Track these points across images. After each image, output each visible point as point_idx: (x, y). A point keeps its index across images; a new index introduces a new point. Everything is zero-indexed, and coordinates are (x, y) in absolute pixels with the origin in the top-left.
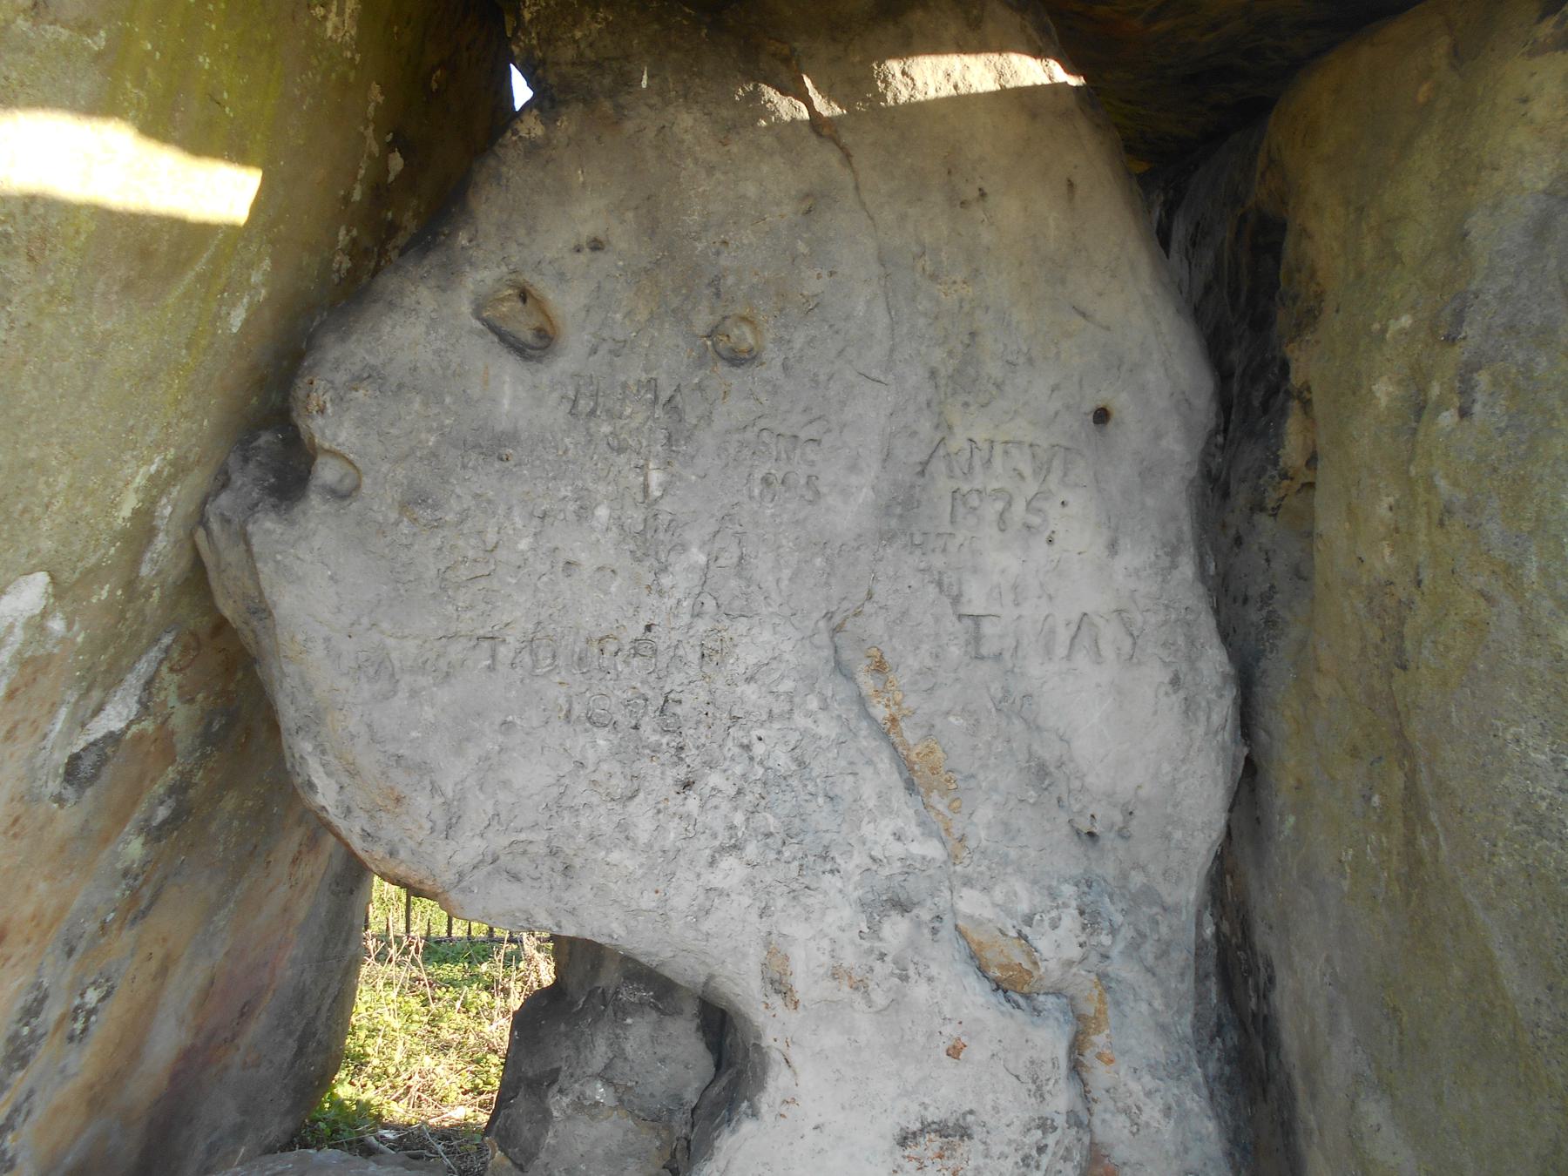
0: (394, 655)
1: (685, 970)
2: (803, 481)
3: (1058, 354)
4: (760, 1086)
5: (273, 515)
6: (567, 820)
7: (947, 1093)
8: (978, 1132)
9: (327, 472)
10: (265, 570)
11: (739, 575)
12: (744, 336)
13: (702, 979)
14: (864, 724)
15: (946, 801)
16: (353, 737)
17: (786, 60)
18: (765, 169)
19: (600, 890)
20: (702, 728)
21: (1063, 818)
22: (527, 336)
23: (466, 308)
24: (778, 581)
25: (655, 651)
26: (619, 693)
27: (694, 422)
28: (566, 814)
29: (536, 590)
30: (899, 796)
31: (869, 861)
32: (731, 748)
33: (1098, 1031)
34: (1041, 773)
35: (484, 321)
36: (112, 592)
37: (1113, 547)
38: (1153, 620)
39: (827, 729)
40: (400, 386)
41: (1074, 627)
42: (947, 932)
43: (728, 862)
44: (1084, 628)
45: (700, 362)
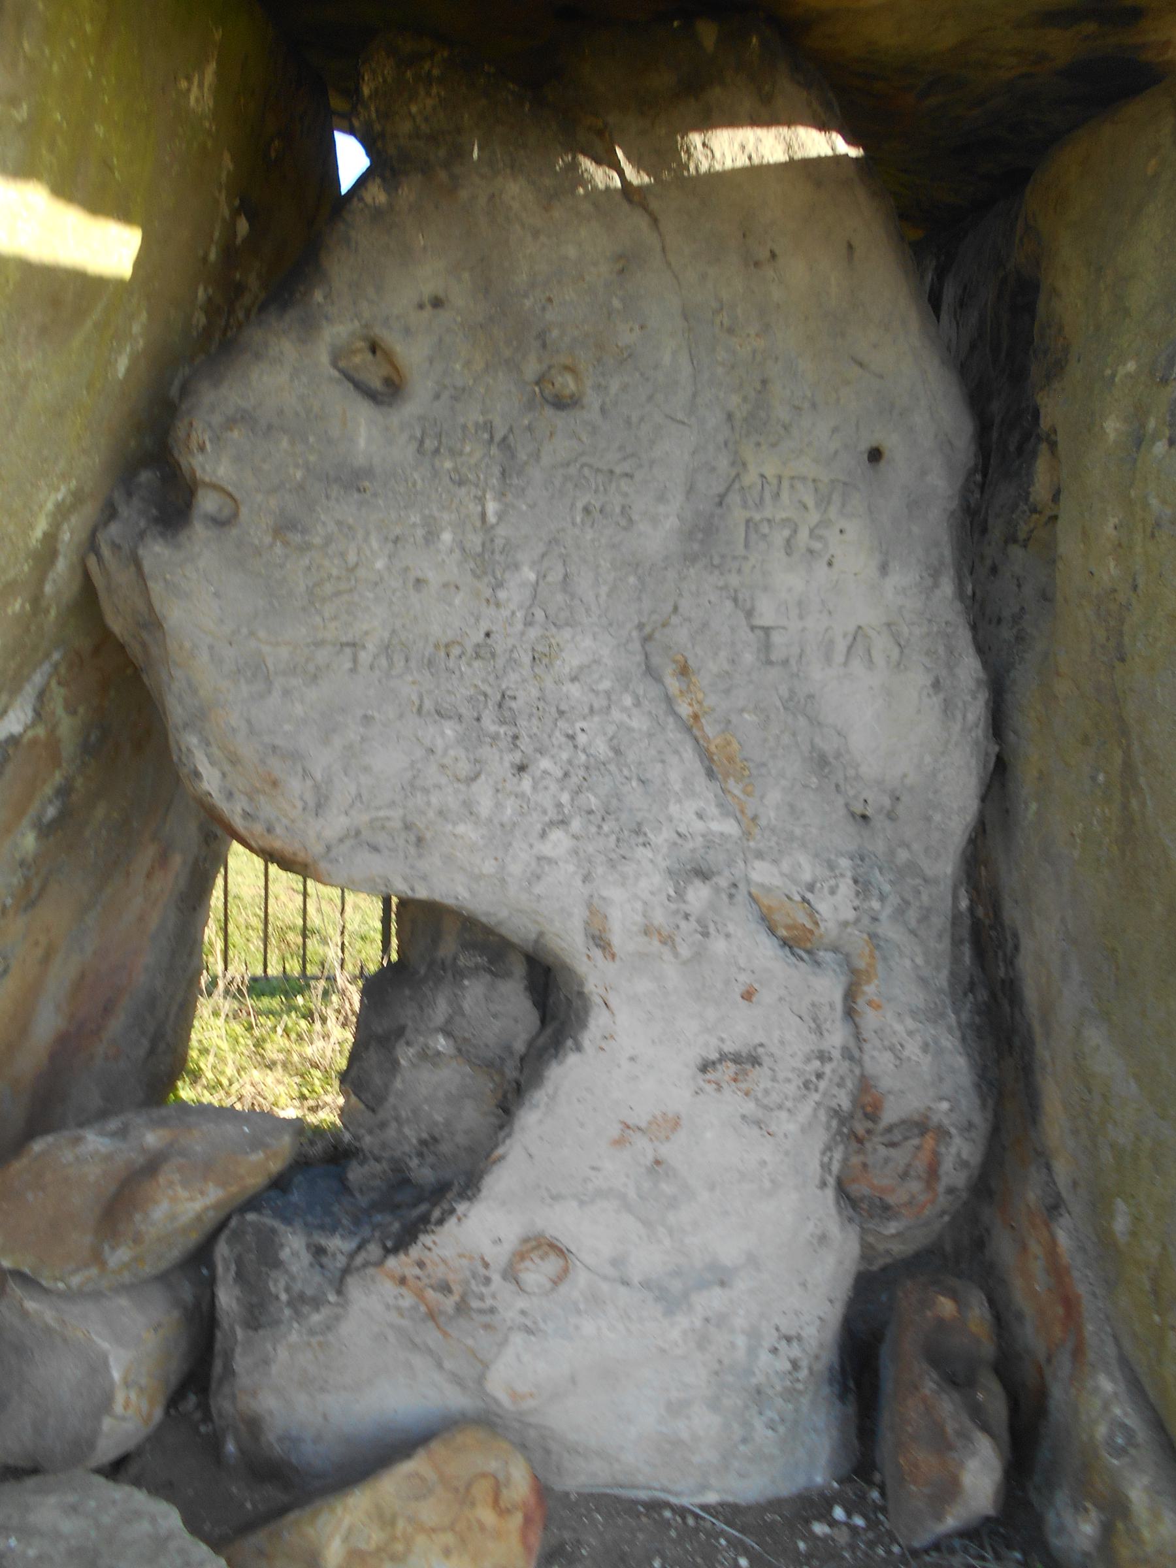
0: (270, 662)
1: (520, 929)
2: (618, 510)
3: (838, 399)
4: (583, 1024)
5: (160, 540)
6: (420, 799)
7: (741, 1030)
8: (766, 1061)
9: (207, 503)
10: (156, 588)
11: (565, 591)
12: (569, 384)
13: (533, 936)
14: (671, 720)
15: (741, 786)
16: (233, 730)
17: (600, 133)
18: (583, 232)
19: (448, 859)
20: (535, 721)
21: (840, 801)
22: (377, 384)
23: (325, 359)
24: (597, 596)
25: (493, 655)
26: (463, 691)
27: (525, 458)
28: (419, 794)
29: (391, 603)
30: (701, 781)
31: (675, 836)
32: (559, 738)
33: (868, 982)
34: (821, 762)
35: (341, 371)
36: (22, 606)
37: (884, 569)
38: (917, 631)
39: (639, 723)
40: (270, 427)
41: (850, 638)
42: (741, 896)
43: (556, 835)
44: (859, 638)
45: (530, 405)
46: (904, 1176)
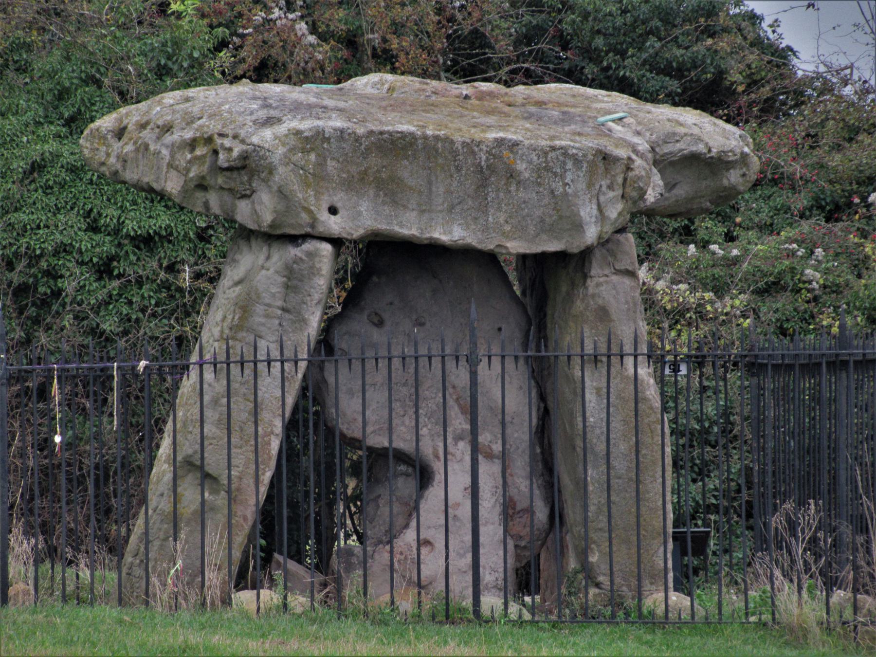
4: (434, 480)
30: (460, 415)
46: (525, 526)
